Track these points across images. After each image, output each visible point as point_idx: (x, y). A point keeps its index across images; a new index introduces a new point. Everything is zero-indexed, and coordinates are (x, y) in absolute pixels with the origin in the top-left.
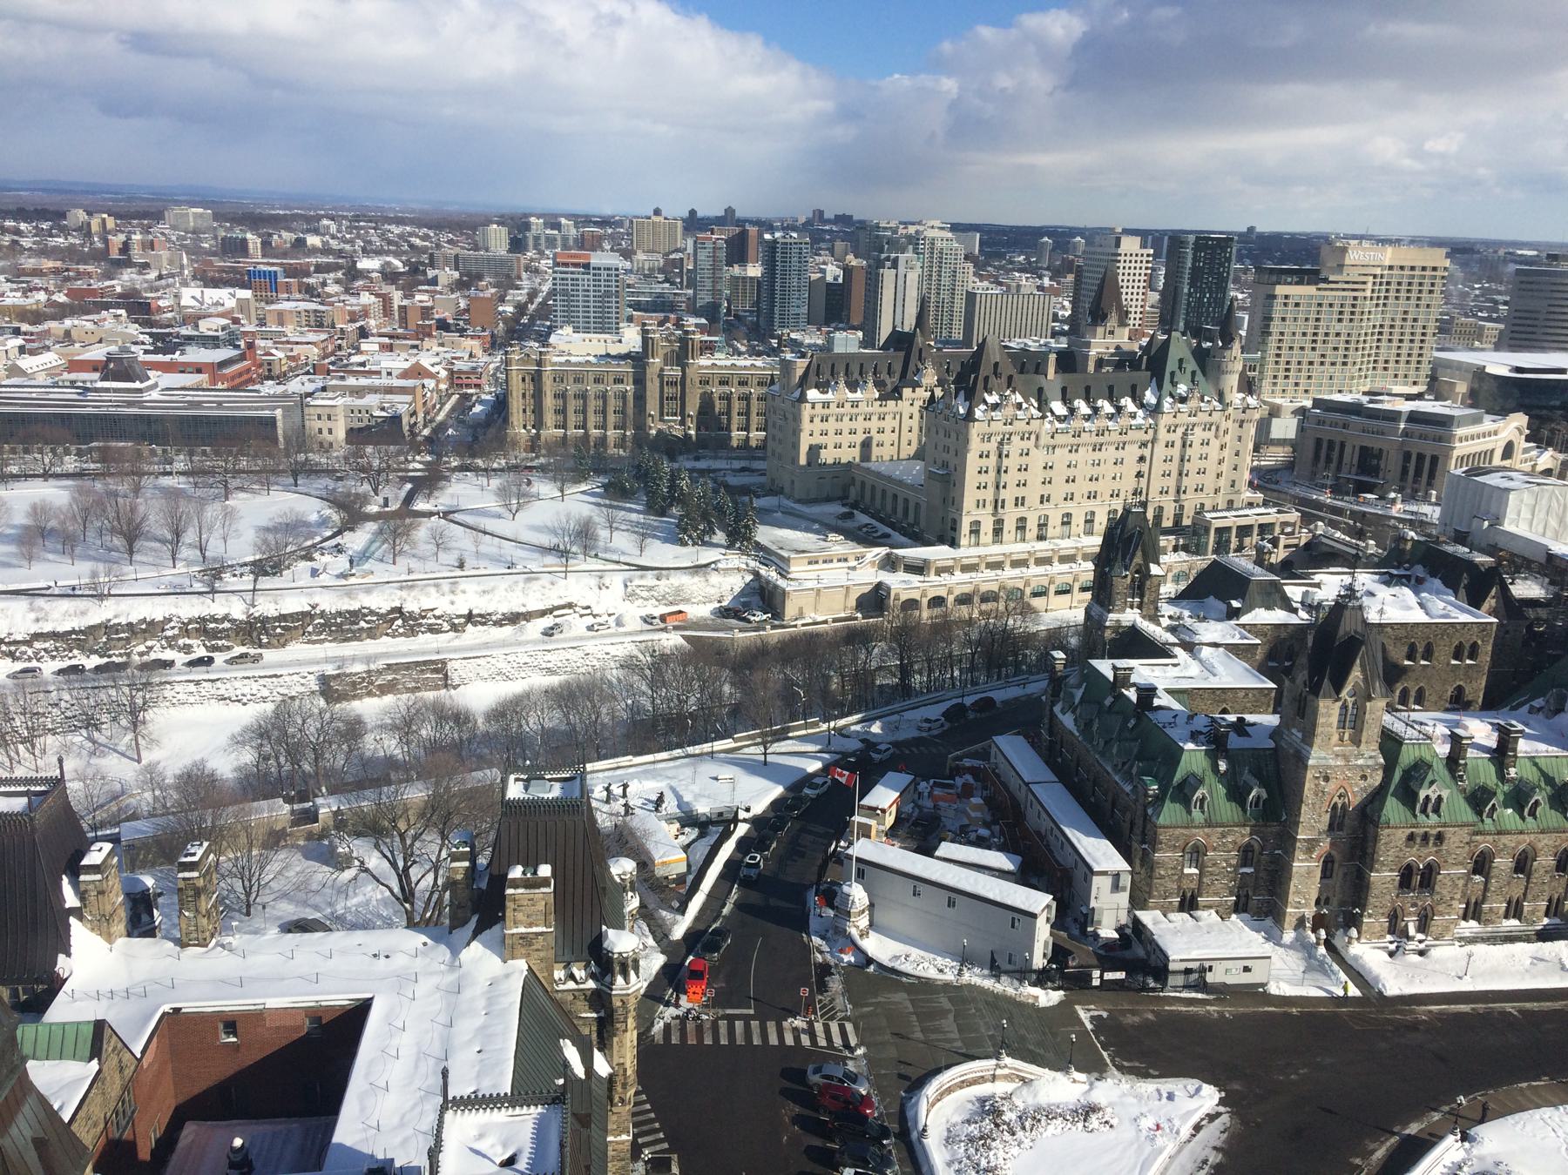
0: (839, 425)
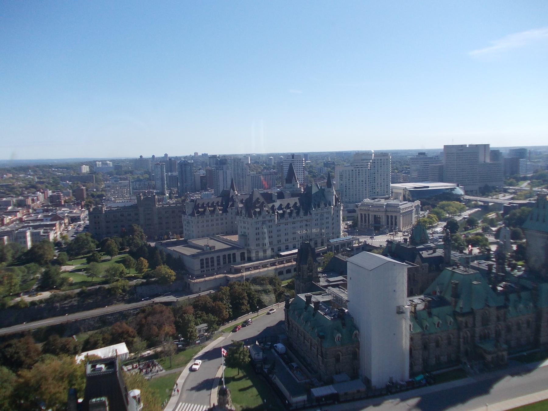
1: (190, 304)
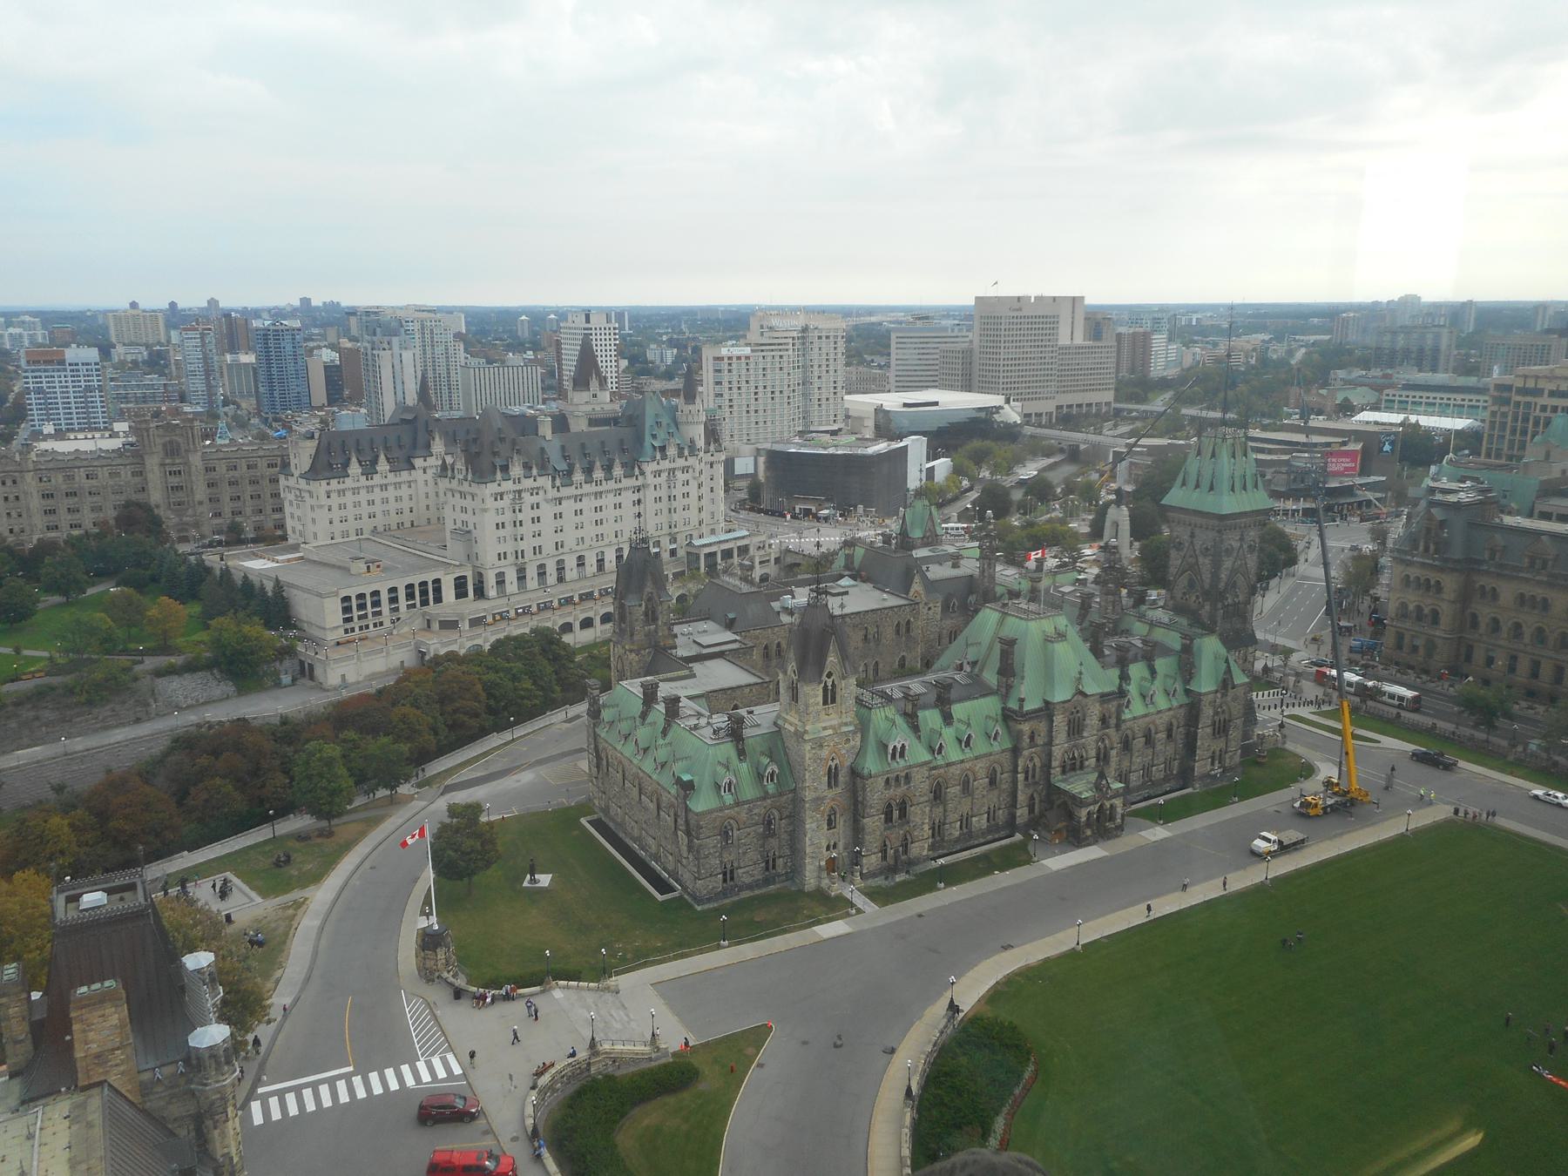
0: (342, 500)
1: (67, 808)
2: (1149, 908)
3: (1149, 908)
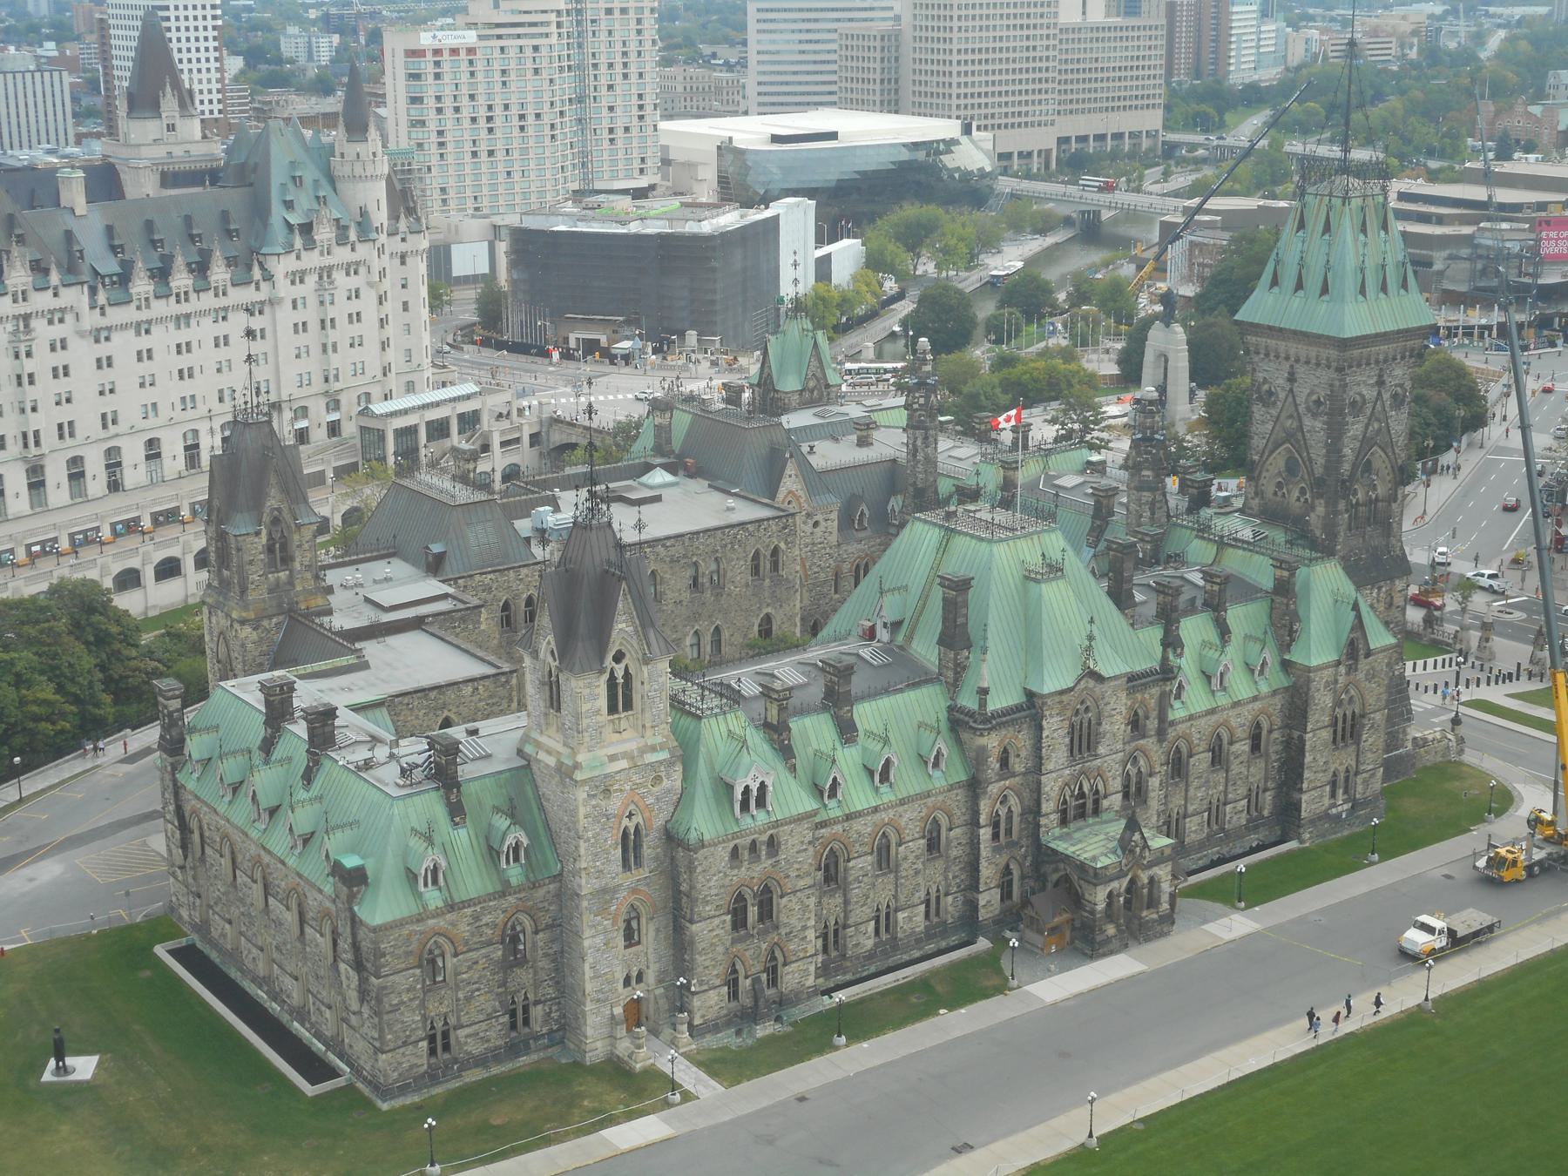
2: (1378, 1003)
3: (1378, 1003)
